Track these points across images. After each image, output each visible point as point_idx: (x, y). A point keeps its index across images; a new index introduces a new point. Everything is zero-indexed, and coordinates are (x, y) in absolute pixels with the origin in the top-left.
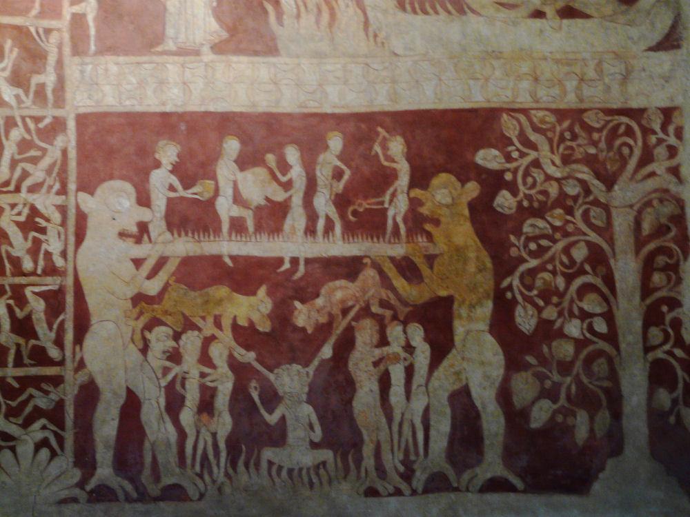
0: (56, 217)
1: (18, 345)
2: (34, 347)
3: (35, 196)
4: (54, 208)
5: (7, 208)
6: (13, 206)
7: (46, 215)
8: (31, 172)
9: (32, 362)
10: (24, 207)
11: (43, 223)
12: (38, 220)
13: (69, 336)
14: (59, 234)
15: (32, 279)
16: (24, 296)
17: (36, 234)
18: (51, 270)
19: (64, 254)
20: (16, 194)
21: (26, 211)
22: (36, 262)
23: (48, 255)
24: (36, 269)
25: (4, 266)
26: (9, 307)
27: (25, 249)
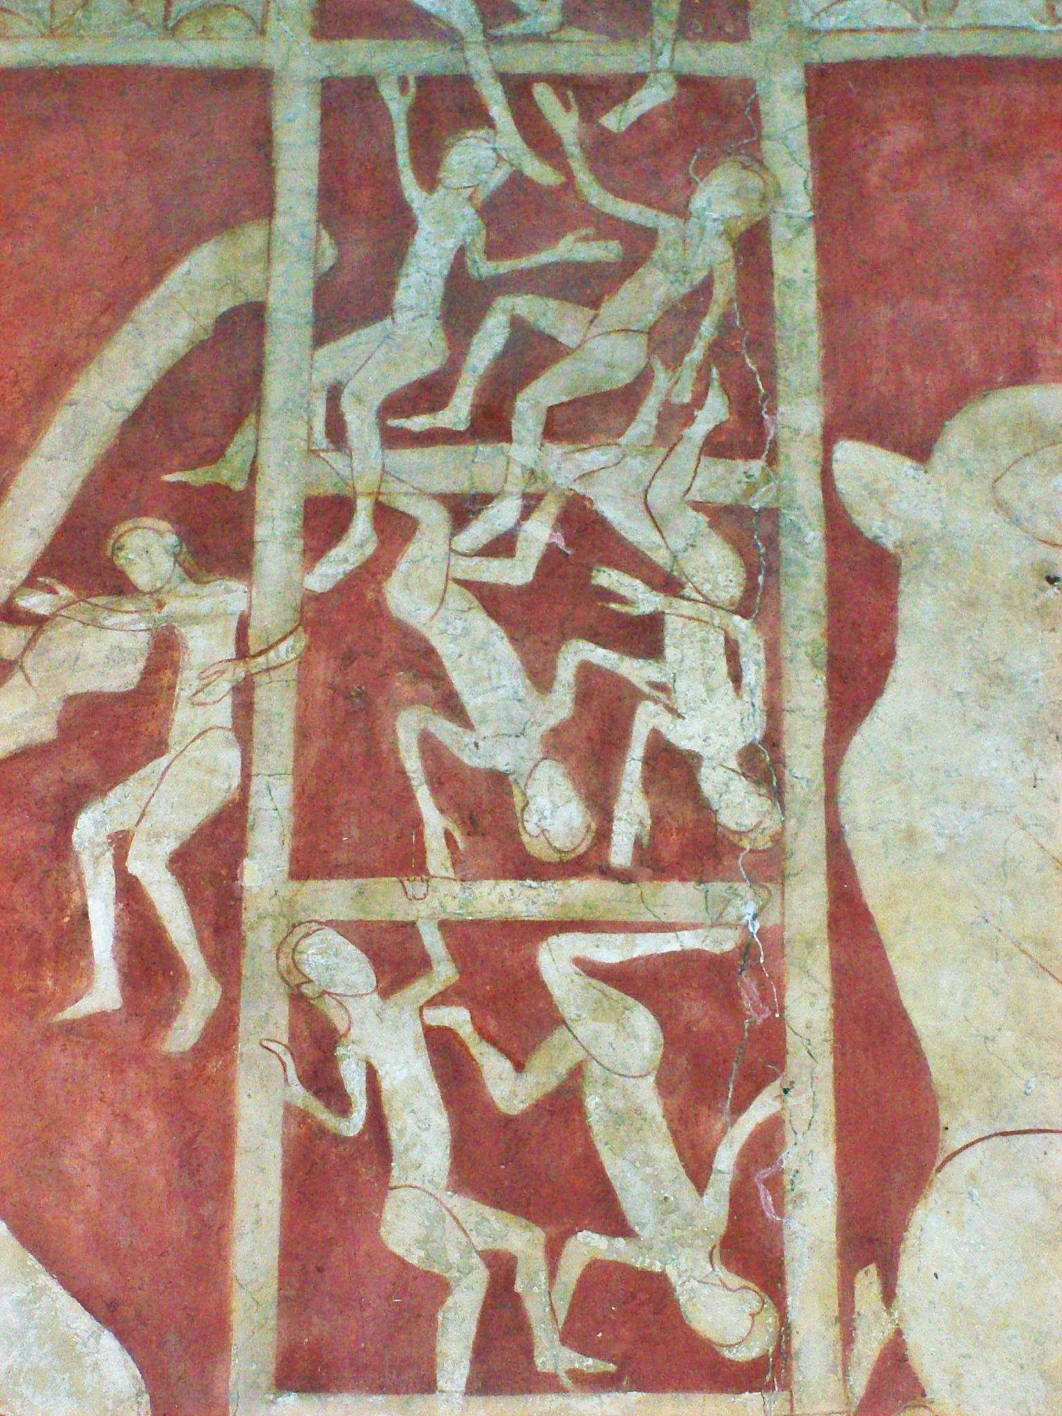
0: (716, 567)
1: (502, 1270)
2: (599, 1276)
3: (594, 458)
4: (703, 519)
5: (433, 518)
6: (462, 510)
7: (661, 557)
8: (568, 338)
9: (590, 1364)
10: (526, 513)
11: (643, 599)
12: (607, 578)
13: (811, 1224)
14: (732, 652)
15: (582, 892)
16: (534, 976)
17: (601, 656)
18: (691, 846)
19: (763, 763)
20: (485, 449)
21: (540, 532)
22: (601, 802)
23: (672, 768)
24: (603, 836)
25: (417, 823)
26: (445, 1052)
27: (536, 733)
